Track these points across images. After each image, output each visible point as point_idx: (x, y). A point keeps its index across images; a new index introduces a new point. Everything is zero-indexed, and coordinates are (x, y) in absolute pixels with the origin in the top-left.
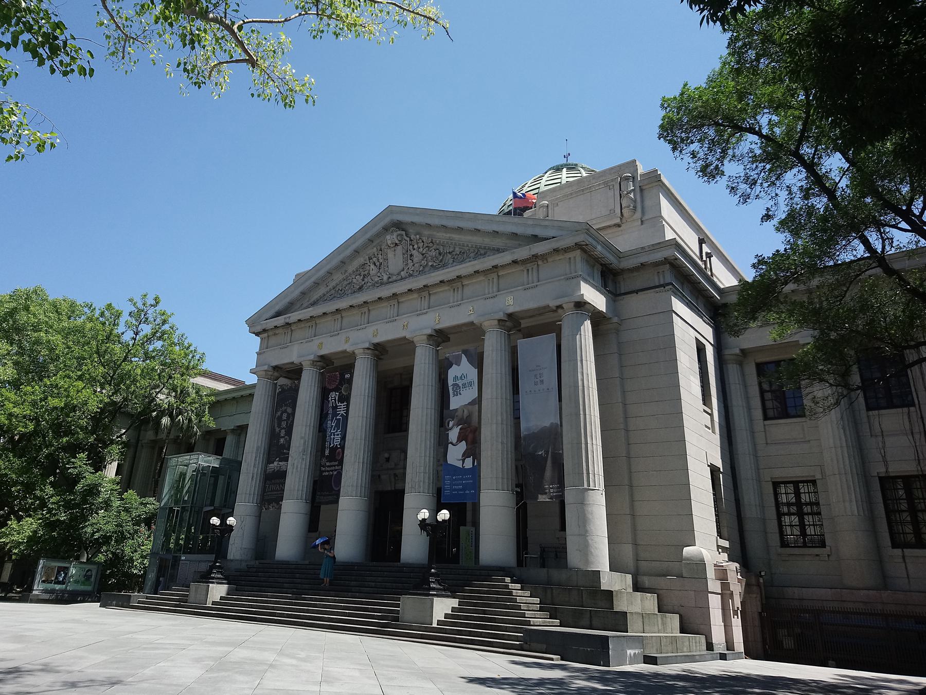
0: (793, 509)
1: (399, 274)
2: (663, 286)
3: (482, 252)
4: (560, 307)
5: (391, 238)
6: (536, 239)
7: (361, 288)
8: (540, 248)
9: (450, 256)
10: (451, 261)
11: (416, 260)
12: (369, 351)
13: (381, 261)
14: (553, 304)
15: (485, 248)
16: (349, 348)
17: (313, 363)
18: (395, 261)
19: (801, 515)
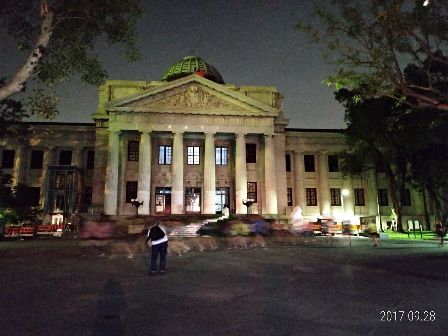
1: (196, 104)
4: (267, 136)
8: (263, 114)
15: (238, 106)
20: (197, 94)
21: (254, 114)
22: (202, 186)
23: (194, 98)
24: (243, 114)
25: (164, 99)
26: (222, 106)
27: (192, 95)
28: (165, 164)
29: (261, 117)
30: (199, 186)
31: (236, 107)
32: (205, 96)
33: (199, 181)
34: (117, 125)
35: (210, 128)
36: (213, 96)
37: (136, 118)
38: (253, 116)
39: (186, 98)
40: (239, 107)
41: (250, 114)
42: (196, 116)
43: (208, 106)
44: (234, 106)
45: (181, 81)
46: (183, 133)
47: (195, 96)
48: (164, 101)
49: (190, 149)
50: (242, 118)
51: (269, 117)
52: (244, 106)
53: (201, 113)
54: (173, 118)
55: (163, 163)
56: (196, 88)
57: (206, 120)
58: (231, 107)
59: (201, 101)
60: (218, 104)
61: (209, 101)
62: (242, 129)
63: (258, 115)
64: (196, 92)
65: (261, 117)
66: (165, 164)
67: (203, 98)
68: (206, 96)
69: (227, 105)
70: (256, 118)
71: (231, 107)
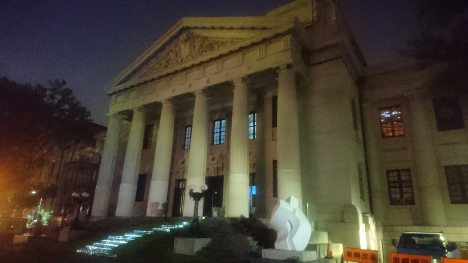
0: (397, 185)
1: (187, 57)
2: (337, 58)
3: (235, 41)
4: (278, 68)
5: (183, 37)
6: (265, 28)
7: (166, 67)
8: (267, 34)
9: (216, 45)
10: (217, 47)
11: (196, 48)
13: (177, 50)
14: (273, 66)
15: (236, 38)
17: (140, 109)
18: (185, 50)
19: (401, 187)
20: (187, 44)
21: (255, 40)
22: (224, 173)
23: (185, 50)
25: (157, 63)
27: (182, 46)
29: (266, 41)
30: (220, 174)
31: (235, 41)
32: (197, 41)
33: (220, 165)
35: (197, 83)
36: (207, 38)
37: (133, 94)
38: (253, 45)
40: (238, 39)
42: (184, 73)
44: (232, 41)
46: (169, 100)
49: (217, 123)
52: (245, 34)
54: (162, 83)
58: (229, 44)
59: (193, 50)
60: (211, 47)
62: (235, 70)
64: (186, 41)
65: (266, 41)
67: (194, 47)
68: (198, 42)
69: (224, 43)
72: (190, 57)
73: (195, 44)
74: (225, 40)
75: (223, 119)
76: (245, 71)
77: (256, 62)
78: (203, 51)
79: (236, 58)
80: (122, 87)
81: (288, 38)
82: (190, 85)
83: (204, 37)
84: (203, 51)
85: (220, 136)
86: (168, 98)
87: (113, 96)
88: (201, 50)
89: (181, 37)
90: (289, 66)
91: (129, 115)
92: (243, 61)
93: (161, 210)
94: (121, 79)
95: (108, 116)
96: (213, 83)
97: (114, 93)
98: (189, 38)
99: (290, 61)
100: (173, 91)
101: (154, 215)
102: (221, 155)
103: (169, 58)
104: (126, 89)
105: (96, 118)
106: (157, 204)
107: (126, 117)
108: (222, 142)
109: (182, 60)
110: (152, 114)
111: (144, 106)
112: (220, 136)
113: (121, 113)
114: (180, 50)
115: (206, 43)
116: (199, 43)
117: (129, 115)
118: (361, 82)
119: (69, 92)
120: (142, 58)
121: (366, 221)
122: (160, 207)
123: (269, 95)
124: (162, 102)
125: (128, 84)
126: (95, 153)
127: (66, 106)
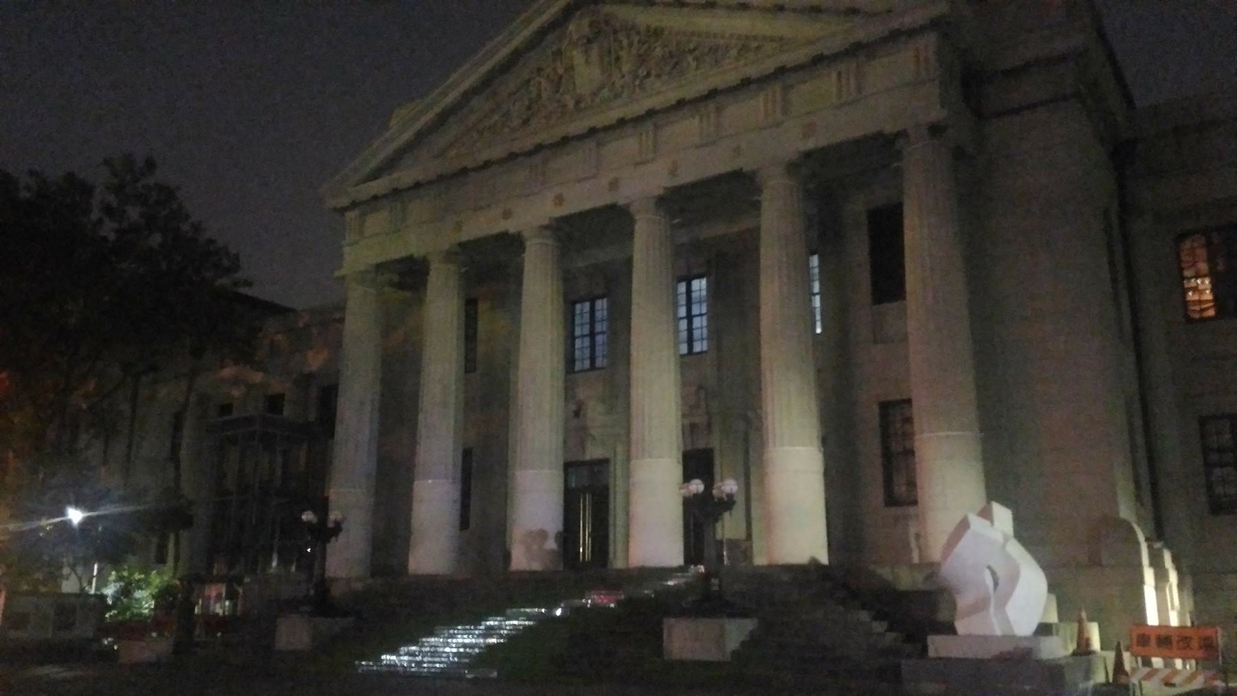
1: (595, 94)
3: (755, 44)
4: (902, 134)
9: (690, 58)
11: (626, 68)
12: (548, 233)
13: (561, 71)
14: (889, 129)
15: (755, 38)
16: (511, 226)
17: (449, 256)
20: (595, 50)
23: (587, 72)
24: (769, 66)
25: (493, 111)
26: (694, 64)
27: (577, 56)
28: (593, 367)
29: (855, 50)
30: (701, 445)
32: (625, 42)
34: (367, 248)
35: (637, 176)
36: (657, 33)
37: (419, 209)
38: (818, 60)
39: (557, 83)
40: (765, 38)
41: (800, 55)
42: (591, 143)
43: (637, 83)
44: (746, 45)
45: (529, 21)
46: (546, 227)
47: (587, 62)
48: (496, 117)
50: (777, 87)
51: (895, 36)
53: (599, 120)
55: (587, 364)
56: (585, 22)
57: (629, 144)
60: (675, 62)
61: (642, 59)
62: (765, 138)
63: (836, 44)
64: (589, 41)
66: (593, 367)
67: (618, 59)
68: (631, 45)
69: (714, 52)
70: (842, 67)
71: (734, 52)
72: (605, 93)
73: (623, 54)
74: (722, 42)
75: (700, 276)
76: (794, 141)
77: (830, 114)
78: (648, 75)
79: (761, 98)
80: (380, 186)
81: (929, 42)
82: (614, 185)
83: (648, 29)
84: (648, 75)
85: (690, 330)
86: (546, 222)
87: (351, 215)
88: (642, 72)
89: (572, 27)
90: (936, 130)
91: (410, 275)
92: (785, 111)
93: (553, 551)
94: (374, 163)
95: (343, 278)
96: (687, 176)
97: (354, 205)
98: (599, 32)
99: (936, 114)
100: (559, 200)
101: (536, 566)
102: (700, 387)
103: (534, 95)
104: (396, 193)
105: (264, 277)
106: (543, 535)
107: (396, 278)
108: (697, 348)
109: (577, 103)
110: (489, 272)
111: (460, 244)
112: (690, 330)
113: (380, 267)
114: (570, 68)
115: (658, 51)
116: (634, 51)
117: (410, 275)
118: (1122, 154)
119: (167, 193)
120: (444, 94)
121: (1156, 563)
122: (551, 544)
123: (857, 207)
124: (526, 234)
125: (405, 176)
126: (250, 386)
127: (156, 239)
